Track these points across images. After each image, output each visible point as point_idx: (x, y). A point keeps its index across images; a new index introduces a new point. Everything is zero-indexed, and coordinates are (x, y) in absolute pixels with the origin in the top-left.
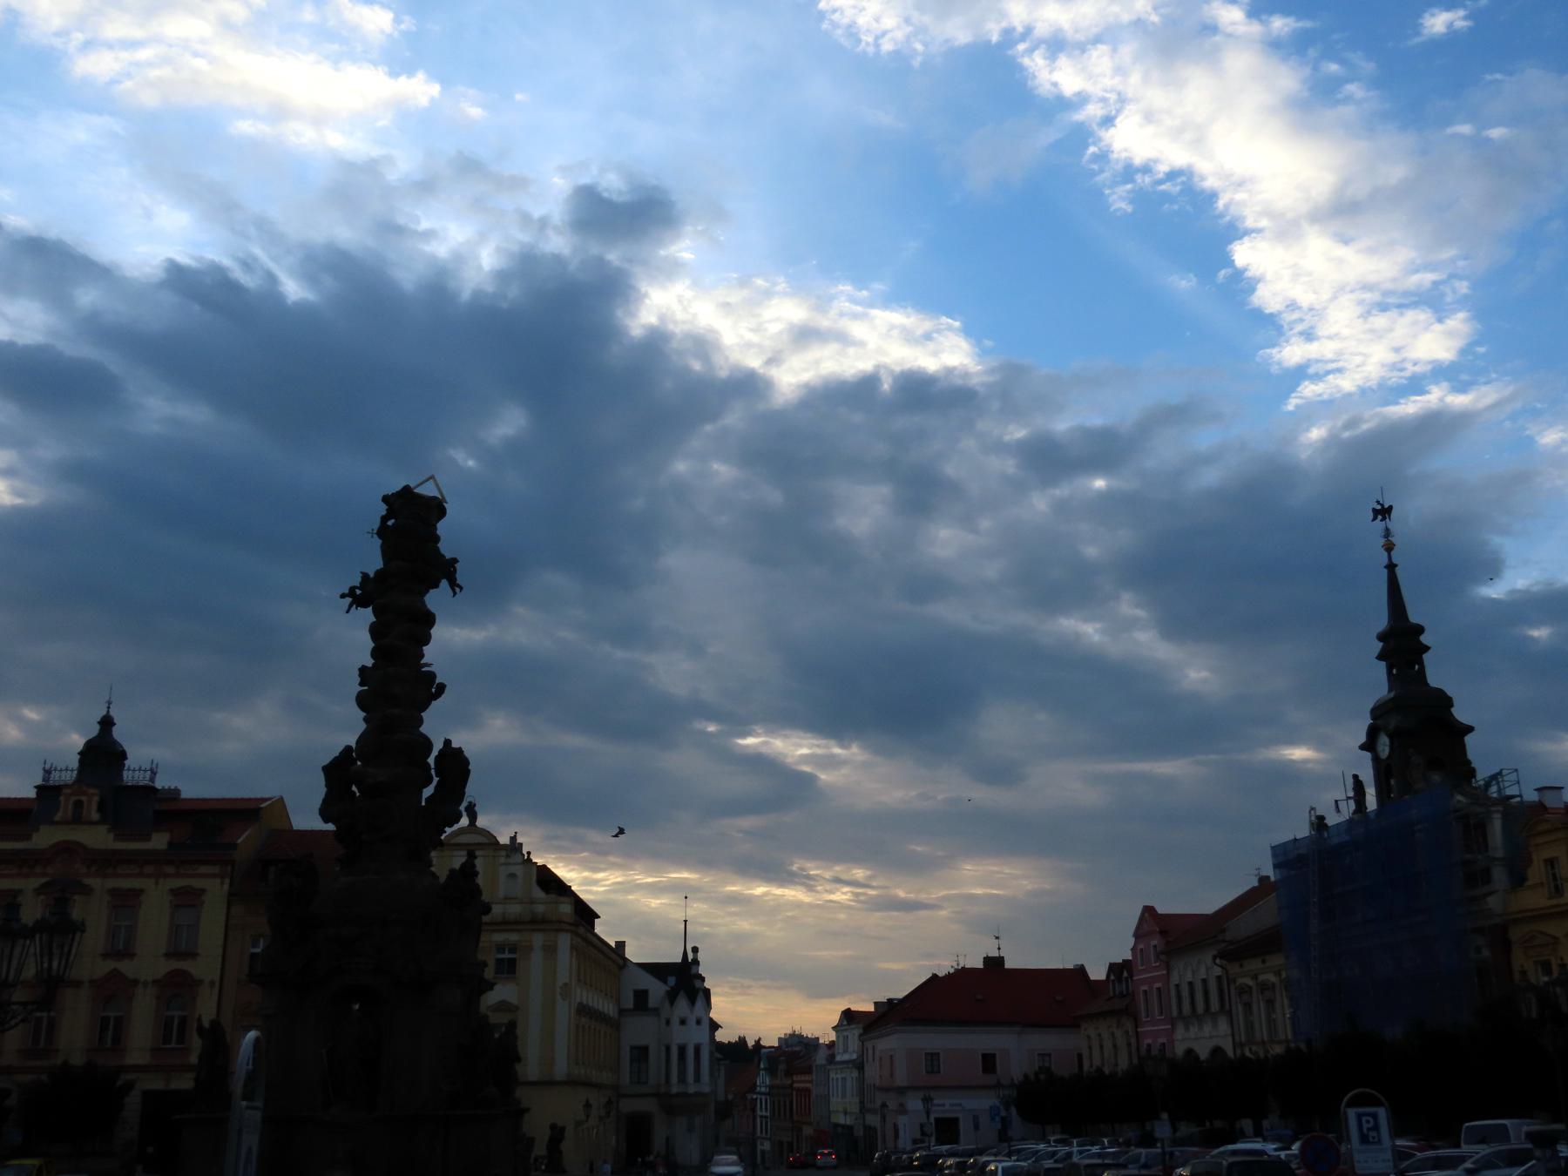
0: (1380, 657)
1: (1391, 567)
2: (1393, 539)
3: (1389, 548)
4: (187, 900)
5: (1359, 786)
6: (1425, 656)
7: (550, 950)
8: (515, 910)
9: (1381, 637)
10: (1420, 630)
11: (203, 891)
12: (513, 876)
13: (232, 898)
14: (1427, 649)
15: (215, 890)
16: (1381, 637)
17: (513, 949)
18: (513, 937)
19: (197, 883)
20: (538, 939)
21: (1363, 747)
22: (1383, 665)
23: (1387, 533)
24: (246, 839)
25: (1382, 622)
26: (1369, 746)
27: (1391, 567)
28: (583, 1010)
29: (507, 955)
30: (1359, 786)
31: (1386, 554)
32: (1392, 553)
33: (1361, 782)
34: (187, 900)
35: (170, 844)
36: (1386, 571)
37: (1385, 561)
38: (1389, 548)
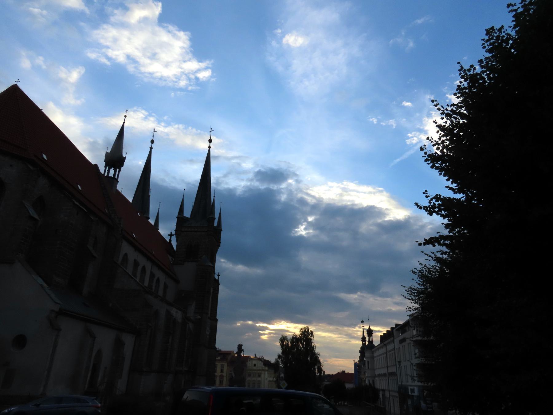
4: (222, 366)
7: (265, 374)
8: (261, 368)
11: (224, 365)
12: (260, 364)
13: (228, 365)
15: (226, 365)
17: (260, 373)
18: (260, 372)
19: (223, 364)
20: (263, 372)
24: (229, 358)
28: (269, 381)
29: (259, 374)
34: (222, 366)
35: (221, 359)
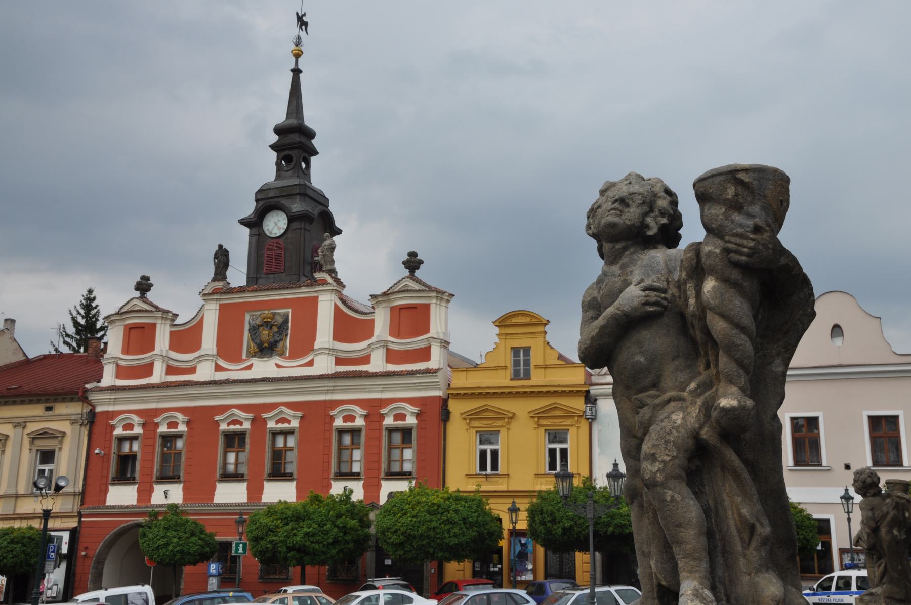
0: (273, 147)
1: (296, 72)
2: (302, 48)
3: (297, 56)
5: (222, 259)
6: (313, 159)
9: (278, 130)
10: (311, 134)
14: (315, 153)
16: (278, 130)
21: (244, 222)
22: (275, 154)
23: (298, 42)
25: (280, 115)
26: (254, 223)
27: (296, 72)
30: (222, 259)
31: (294, 59)
32: (299, 59)
33: (227, 251)
36: (291, 74)
37: (293, 66)
38: (297, 56)
